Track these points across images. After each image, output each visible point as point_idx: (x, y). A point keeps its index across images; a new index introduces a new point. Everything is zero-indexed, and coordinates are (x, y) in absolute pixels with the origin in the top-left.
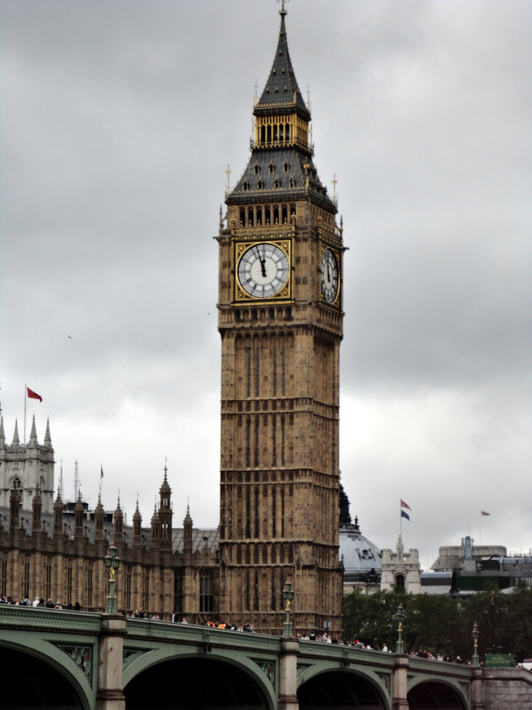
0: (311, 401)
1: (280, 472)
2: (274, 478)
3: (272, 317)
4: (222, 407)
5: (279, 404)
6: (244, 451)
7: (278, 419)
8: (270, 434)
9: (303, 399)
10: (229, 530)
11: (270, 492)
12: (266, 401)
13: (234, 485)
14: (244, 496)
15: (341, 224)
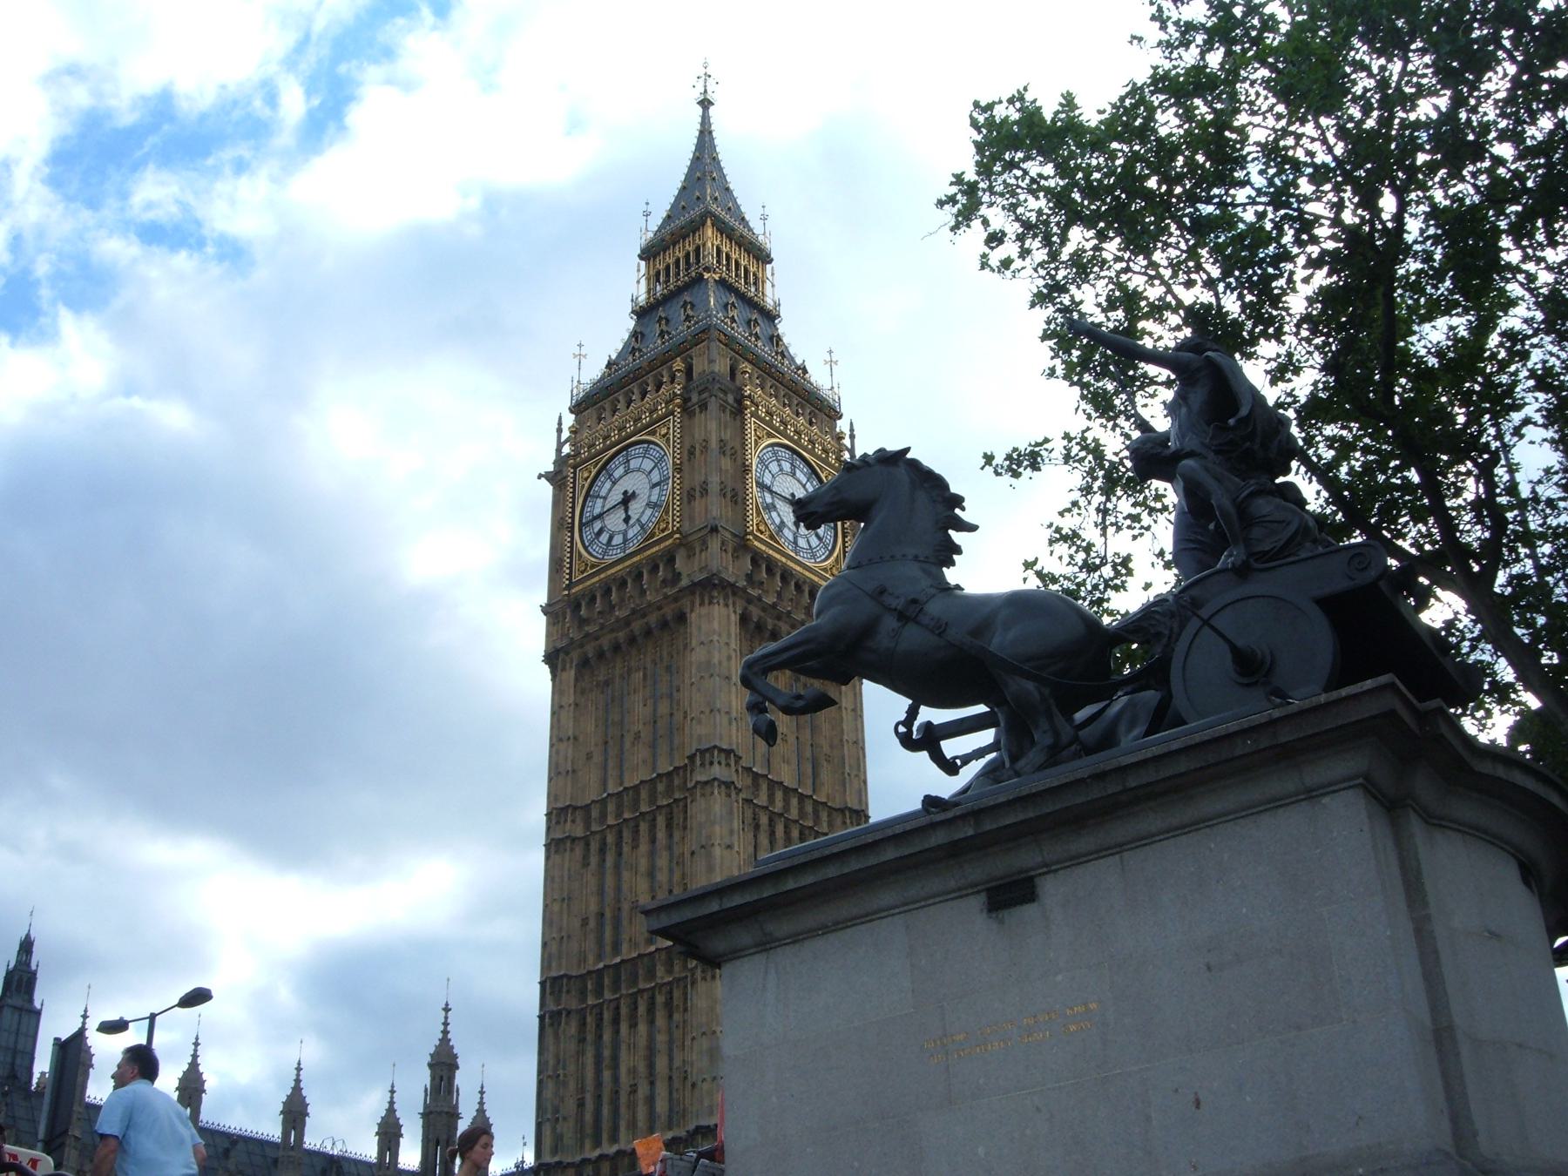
0: (727, 757)
1: (663, 956)
2: (651, 974)
3: (643, 592)
4: (548, 829)
5: (661, 787)
6: (592, 924)
7: (661, 821)
8: (643, 863)
9: (703, 752)
10: (554, 1129)
11: (642, 1009)
12: (636, 788)
13: (569, 1013)
14: (590, 1037)
15: (852, 437)
